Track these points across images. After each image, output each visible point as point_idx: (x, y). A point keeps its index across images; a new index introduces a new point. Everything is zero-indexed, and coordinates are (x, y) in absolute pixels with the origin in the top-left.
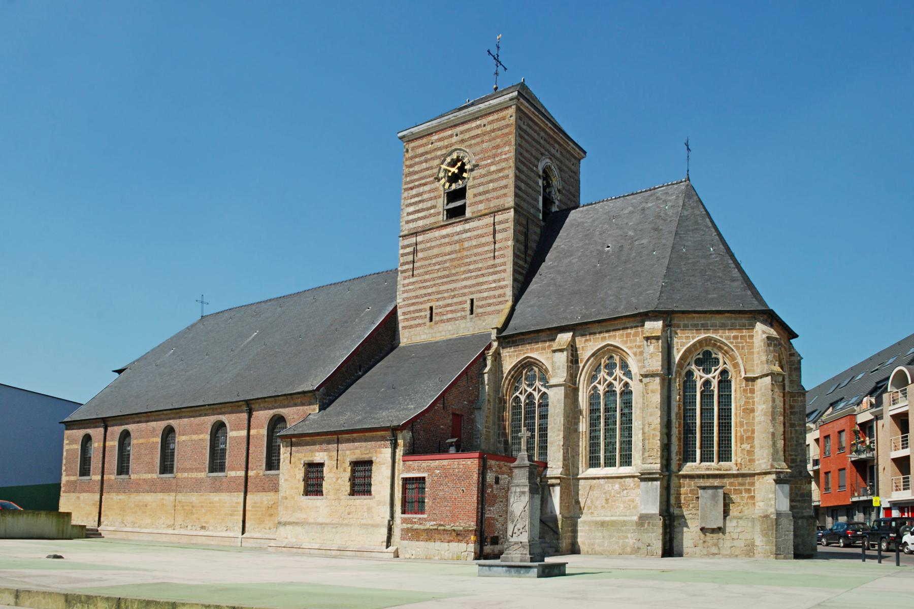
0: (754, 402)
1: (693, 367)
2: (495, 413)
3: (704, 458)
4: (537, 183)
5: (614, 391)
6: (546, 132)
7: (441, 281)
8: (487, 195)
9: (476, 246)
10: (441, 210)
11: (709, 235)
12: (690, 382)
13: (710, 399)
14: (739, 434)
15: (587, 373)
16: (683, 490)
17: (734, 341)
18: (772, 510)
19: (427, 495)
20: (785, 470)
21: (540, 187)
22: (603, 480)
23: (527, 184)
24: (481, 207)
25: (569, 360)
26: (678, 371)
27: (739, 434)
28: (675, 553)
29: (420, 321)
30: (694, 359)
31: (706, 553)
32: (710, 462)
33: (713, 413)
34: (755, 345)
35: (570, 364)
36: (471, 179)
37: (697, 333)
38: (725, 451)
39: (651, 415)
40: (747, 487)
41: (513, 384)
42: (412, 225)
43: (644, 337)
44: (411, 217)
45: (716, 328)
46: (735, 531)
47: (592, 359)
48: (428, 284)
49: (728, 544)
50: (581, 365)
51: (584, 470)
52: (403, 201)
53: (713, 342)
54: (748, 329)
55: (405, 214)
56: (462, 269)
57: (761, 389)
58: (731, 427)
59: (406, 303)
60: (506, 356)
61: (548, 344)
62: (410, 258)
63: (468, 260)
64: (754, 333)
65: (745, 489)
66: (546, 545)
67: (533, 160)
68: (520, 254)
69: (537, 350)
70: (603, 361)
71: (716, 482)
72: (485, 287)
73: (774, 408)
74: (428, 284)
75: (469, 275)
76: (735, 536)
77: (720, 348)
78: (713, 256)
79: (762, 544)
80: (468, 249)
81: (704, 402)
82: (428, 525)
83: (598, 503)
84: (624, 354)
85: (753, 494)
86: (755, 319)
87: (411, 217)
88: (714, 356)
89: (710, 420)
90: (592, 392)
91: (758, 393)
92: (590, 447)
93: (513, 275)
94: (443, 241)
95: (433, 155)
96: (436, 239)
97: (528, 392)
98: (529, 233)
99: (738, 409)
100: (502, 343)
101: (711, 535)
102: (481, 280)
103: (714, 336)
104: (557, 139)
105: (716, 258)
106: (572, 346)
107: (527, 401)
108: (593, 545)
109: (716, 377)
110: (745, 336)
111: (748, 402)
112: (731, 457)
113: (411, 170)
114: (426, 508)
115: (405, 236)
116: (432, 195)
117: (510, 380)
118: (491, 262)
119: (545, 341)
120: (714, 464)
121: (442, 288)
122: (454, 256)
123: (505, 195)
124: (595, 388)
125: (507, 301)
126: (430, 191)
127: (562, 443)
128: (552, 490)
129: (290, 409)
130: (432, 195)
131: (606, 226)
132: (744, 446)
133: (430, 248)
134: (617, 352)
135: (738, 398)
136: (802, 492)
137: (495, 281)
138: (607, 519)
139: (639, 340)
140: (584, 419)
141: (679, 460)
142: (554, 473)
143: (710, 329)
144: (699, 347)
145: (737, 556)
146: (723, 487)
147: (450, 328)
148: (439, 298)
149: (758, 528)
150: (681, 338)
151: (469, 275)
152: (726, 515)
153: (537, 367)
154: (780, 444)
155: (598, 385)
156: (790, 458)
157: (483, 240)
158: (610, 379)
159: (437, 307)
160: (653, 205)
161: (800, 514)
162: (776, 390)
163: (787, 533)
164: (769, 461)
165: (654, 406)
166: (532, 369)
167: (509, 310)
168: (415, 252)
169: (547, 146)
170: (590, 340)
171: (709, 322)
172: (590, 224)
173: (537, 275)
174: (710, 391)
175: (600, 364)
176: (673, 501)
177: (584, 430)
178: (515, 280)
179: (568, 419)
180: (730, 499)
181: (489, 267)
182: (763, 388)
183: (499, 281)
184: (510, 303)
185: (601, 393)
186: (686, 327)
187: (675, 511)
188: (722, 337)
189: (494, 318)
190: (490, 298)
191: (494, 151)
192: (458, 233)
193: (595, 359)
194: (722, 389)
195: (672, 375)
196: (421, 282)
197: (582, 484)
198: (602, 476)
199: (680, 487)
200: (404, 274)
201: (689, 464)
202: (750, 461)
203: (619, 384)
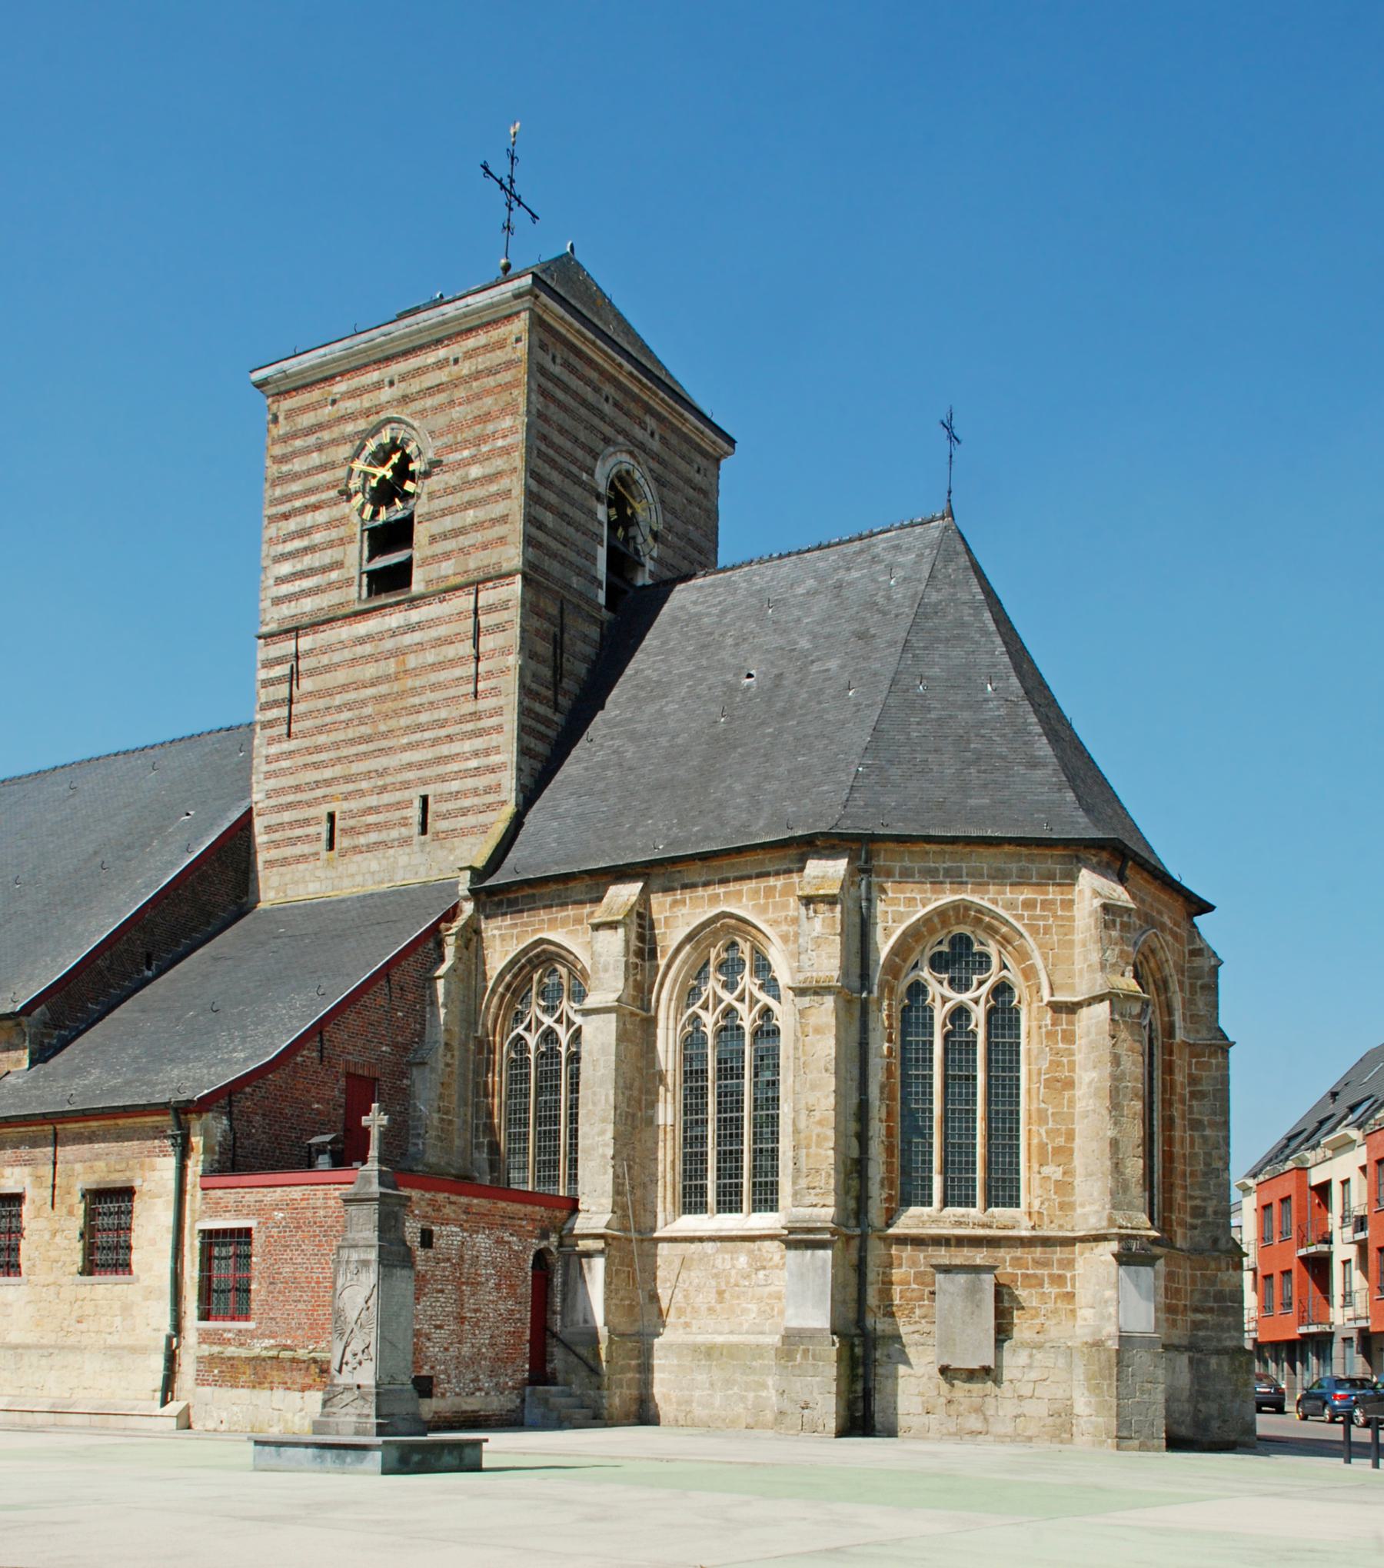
0: (1072, 1064)
1: (926, 974)
2: (464, 1076)
3: (953, 1196)
4: (592, 514)
5: (739, 1027)
6: (619, 385)
7: (354, 750)
8: (461, 538)
9: (437, 666)
10: (354, 572)
11: (987, 652)
12: (917, 1011)
13: (967, 1053)
14: (1035, 1141)
15: (675, 981)
16: (897, 1274)
17: (1026, 914)
18: (1110, 1329)
19: (255, 1273)
20: (1143, 1233)
21: (601, 523)
22: (711, 1244)
23: (562, 516)
24: (447, 568)
25: (632, 948)
26: (887, 981)
27: (1035, 1141)
28: (878, 1427)
30: (928, 953)
31: (953, 1430)
32: (967, 1205)
33: (975, 1086)
34: (1076, 923)
35: (633, 959)
37: (934, 892)
38: (1004, 1180)
39: (814, 1087)
40: (1056, 1271)
41: (510, 1006)
42: (287, 610)
43: (800, 898)
44: (286, 589)
45: (980, 880)
46: (1026, 1378)
47: (688, 948)
48: (324, 756)
49: (1009, 1408)
50: (662, 962)
51: (669, 1219)
52: (265, 547)
53: (973, 913)
54: (1059, 885)
55: (271, 582)
56: (404, 721)
57: (1088, 1033)
58: (1018, 1122)
60: (494, 936)
61: (588, 908)
62: (283, 691)
63: (416, 700)
64: (1076, 896)
65: (1050, 1275)
66: (570, 1400)
67: (580, 453)
68: (543, 691)
69: (564, 923)
70: (713, 956)
71: (980, 1256)
72: (454, 767)
73: (1116, 1078)
74: (324, 756)
75: (418, 736)
76: (1026, 1390)
77: (991, 930)
78: (991, 705)
79: (1088, 1411)
80: (416, 672)
81: (953, 1060)
82: (260, 1347)
83: (702, 1300)
84: (760, 937)
85: (1069, 1289)
86: (1078, 859)
87: (286, 589)
88: (976, 948)
89: (967, 1104)
90: (690, 1029)
91: (1084, 1041)
92: (685, 1164)
93: (519, 739)
94: (359, 650)
96: (343, 645)
97: (544, 1027)
98: (566, 636)
99: (1035, 1078)
100: (484, 905)
101: (967, 1386)
102: (445, 749)
103: (975, 899)
104: (651, 402)
105: (998, 709)
106: (640, 916)
107: (543, 1049)
108: (689, 1402)
109: (982, 1001)
110: (1053, 902)
111: (1059, 1064)
112: (1018, 1197)
114: (254, 1305)
115: (271, 635)
116: (334, 534)
117: (503, 996)
118: (469, 707)
119: (582, 903)
120: (975, 1213)
122: (383, 689)
123: (502, 540)
124: (695, 1018)
125: (504, 803)
126: (330, 525)
127: (611, 1152)
128: (585, 1266)
130: (334, 534)
131: (751, 625)
132: (1047, 1170)
133: (329, 668)
134: (744, 932)
135: (1034, 1052)
136: (1219, 1287)
137: (476, 754)
138: (719, 1339)
139: (794, 907)
140: (669, 1095)
141: (889, 1199)
142: (592, 1223)
143: (966, 883)
144: (939, 926)
145: (1030, 1439)
146: (995, 1268)
147: (374, 866)
148: (350, 793)
149: (1079, 1373)
150: (895, 901)
151: (418, 736)
152: (1001, 1337)
153: (564, 966)
154: (1135, 1167)
155: (701, 1012)
156: (1189, 1203)
157: (451, 652)
158: (728, 998)
160: (863, 577)
161: (1214, 1343)
162: (1124, 1035)
163: (1149, 1386)
164: (1104, 1208)
165: (822, 1064)
166: (555, 970)
167: (507, 824)
168: (294, 677)
169: (623, 421)
170: (683, 902)
171: (964, 865)
172: (715, 619)
173: (582, 742)
174: (968, 1034)
175: (707, 963)
176: (872, 1299)
177: (670, 1122)
178: (524, 752)
179: (628, 1093)
180: (1014, 1298)
181: (463, 719)
182: (1093, 1030)
183: (487, 752)
184: (510, 809)
185: (709, 1031)
186: (906, 875)
187: (878, 1324)
188: (995, 902)
189: (474, 845)
192: (393, 633)
193: (694, 949)
194: (996, 1028)
195: (870, 992)
196: (309, 751)
197: (665, 1252)
198: (708, 1234)
199: (890, 1266)
200: (269, 732)
201: (914, 1210)
202: (1062, 1206)
203: (751, 1011)
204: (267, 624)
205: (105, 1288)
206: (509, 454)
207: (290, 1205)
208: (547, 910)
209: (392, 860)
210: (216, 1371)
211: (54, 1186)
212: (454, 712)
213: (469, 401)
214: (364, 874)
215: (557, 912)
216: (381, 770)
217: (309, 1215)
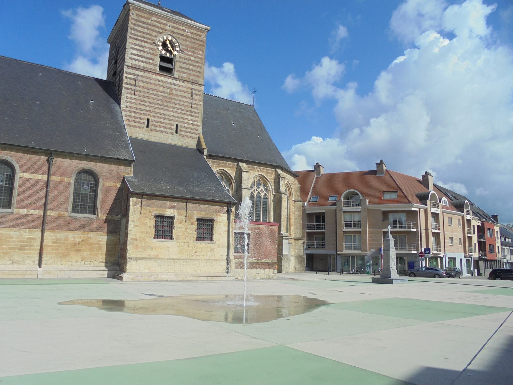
29: (140, 125)
59: (128, 109)
72: (186, 121)
94: (158, 83)
95: (153, 28)
96: (153, 79)
102: (183, 116)
113: (136, 27)
115: (129, 66)
118: (190, 109)
121: (156, 110)
122: (166, 95)
126: (150, 48)
137: (192, 120)
148: (155, 116)
151: (176, 110)
181: (188, 111)
182: (298, 206)
183: (195, 121)
190: (189, 128)
191: (193, 50)
204: (128, 63)
205: (205, 245)
207: (259, 229)
210: (241, 265)
211: (186, 216)
212: (186, 109)
213: (191, 42)
214: (159, 137)
216: (164, 114)
217: (264, 231)
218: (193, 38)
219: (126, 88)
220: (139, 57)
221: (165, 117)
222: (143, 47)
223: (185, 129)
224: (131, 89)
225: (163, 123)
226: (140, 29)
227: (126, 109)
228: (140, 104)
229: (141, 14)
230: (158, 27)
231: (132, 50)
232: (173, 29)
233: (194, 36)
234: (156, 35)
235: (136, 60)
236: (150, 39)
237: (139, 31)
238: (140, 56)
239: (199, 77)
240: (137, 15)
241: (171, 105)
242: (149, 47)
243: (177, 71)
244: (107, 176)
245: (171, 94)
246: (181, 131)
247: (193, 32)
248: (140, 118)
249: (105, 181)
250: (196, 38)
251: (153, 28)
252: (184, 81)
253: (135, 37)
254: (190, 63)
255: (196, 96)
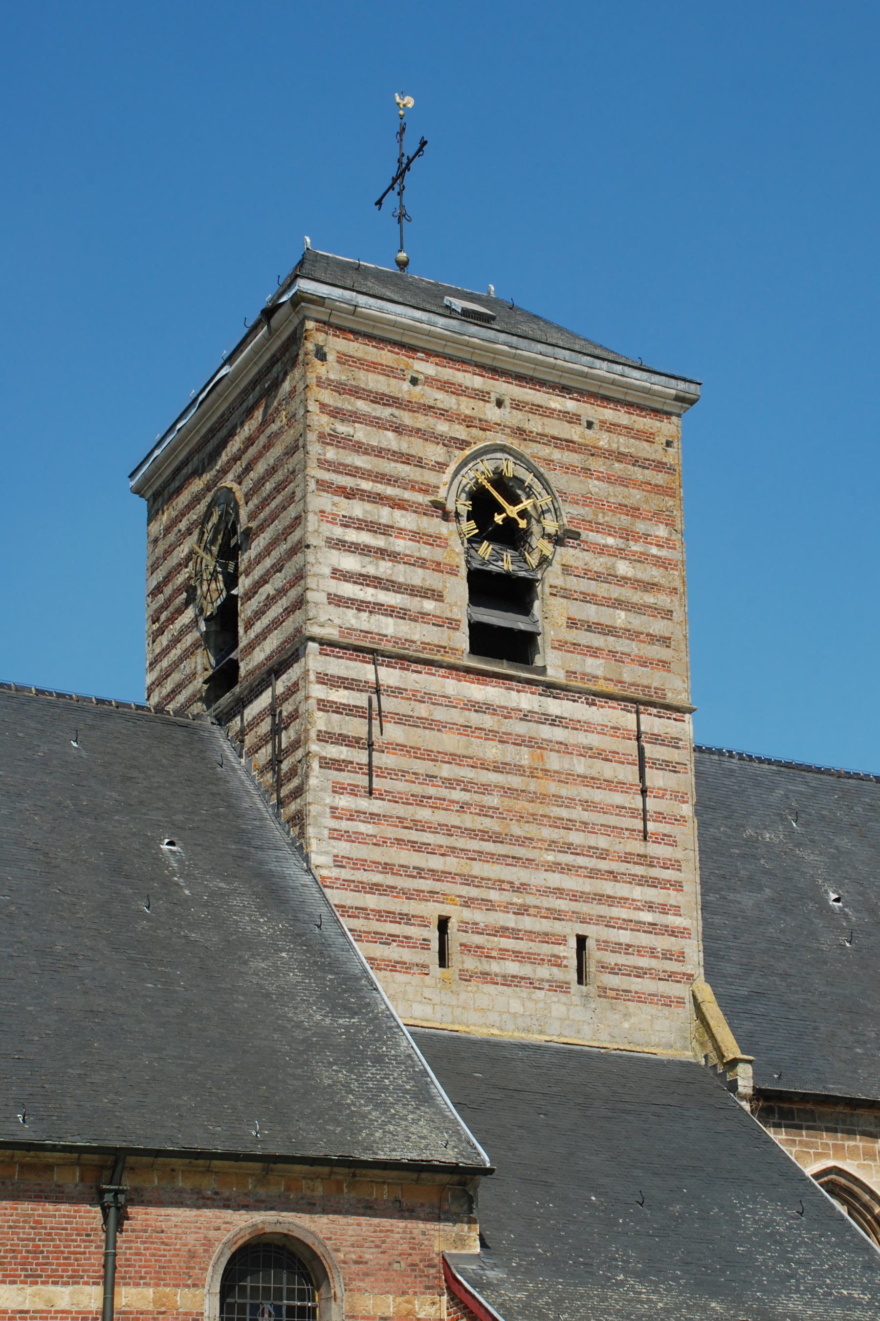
7: (474, 845)
29: (407, 955)
36: (556, 567)
42: (352, 618)
44: (349, 590)
59: (345, 874)
69: (853, 1153)
75: (567, 858)
87: (349, 590)
94: (475, 719)
95: (422, 421)
96: (449, 703)
102: (609, 888)
113: (343, 428)
115: (332, 644)
118: (636, 846)
121: (478, 869)
122: (515, 781)
126: (417, 536)
129: (341, 1219)
137: (650, 906)
147: (516, 1006)
148: (472, 899)
151: (567, 858)
159: (466, 927)
181: (627, 858)
183: (664, 909)
190: (640, 951)
191: (624, 520)
204: (322, 626)
206: (666, 568)
208: (830, 1134)
209: (542, 1005)
214: (501, 1013)
215: (842, 1140)
216: (517, 884)
218: (620, 457)
219: (327, 764)
220: (370, 590)
221: (520, 901)
222: (385, 530)
223: (621, 959)
224: (352, 763)
225: (514, 933)
226: (361, 433)
227: (335, 872)
228: (399, 841)
229: (359, 354)
230: (444, 414)
231: (335, 552)
232: (516, 418)
233: (623, 444)
234: (440, 460)
235: (361, 606)
236: (413, 486)
237: (359, 448)
238: (376, 582)
239: (664, 664)
240: (344, 359)
241: (547, 833)
242: (415, 529)
243: (556, 644)
244: (366, 1263)
245: (540, 774)
246: (603, 967)
247: (616, 421)
248: (405, 918)
249: (359, 1290)
250: (632, 450)
251: (422, 421)
252: (596, 697)
253: (344, 484)
254: (615, 595)
255: (661, 772)
